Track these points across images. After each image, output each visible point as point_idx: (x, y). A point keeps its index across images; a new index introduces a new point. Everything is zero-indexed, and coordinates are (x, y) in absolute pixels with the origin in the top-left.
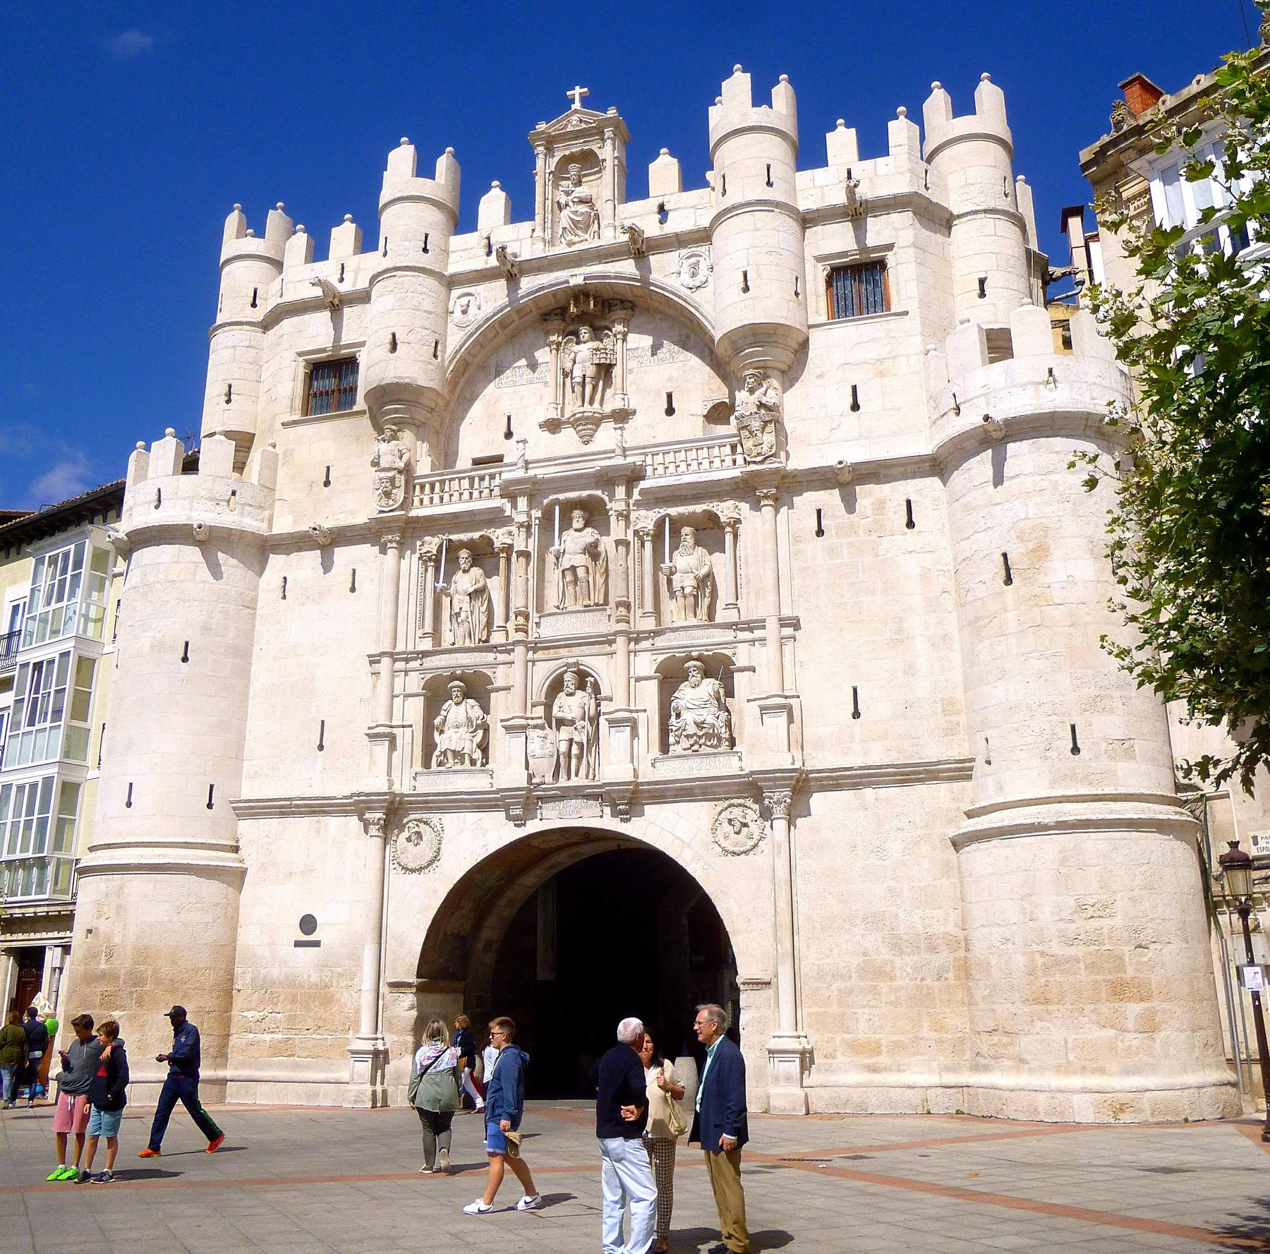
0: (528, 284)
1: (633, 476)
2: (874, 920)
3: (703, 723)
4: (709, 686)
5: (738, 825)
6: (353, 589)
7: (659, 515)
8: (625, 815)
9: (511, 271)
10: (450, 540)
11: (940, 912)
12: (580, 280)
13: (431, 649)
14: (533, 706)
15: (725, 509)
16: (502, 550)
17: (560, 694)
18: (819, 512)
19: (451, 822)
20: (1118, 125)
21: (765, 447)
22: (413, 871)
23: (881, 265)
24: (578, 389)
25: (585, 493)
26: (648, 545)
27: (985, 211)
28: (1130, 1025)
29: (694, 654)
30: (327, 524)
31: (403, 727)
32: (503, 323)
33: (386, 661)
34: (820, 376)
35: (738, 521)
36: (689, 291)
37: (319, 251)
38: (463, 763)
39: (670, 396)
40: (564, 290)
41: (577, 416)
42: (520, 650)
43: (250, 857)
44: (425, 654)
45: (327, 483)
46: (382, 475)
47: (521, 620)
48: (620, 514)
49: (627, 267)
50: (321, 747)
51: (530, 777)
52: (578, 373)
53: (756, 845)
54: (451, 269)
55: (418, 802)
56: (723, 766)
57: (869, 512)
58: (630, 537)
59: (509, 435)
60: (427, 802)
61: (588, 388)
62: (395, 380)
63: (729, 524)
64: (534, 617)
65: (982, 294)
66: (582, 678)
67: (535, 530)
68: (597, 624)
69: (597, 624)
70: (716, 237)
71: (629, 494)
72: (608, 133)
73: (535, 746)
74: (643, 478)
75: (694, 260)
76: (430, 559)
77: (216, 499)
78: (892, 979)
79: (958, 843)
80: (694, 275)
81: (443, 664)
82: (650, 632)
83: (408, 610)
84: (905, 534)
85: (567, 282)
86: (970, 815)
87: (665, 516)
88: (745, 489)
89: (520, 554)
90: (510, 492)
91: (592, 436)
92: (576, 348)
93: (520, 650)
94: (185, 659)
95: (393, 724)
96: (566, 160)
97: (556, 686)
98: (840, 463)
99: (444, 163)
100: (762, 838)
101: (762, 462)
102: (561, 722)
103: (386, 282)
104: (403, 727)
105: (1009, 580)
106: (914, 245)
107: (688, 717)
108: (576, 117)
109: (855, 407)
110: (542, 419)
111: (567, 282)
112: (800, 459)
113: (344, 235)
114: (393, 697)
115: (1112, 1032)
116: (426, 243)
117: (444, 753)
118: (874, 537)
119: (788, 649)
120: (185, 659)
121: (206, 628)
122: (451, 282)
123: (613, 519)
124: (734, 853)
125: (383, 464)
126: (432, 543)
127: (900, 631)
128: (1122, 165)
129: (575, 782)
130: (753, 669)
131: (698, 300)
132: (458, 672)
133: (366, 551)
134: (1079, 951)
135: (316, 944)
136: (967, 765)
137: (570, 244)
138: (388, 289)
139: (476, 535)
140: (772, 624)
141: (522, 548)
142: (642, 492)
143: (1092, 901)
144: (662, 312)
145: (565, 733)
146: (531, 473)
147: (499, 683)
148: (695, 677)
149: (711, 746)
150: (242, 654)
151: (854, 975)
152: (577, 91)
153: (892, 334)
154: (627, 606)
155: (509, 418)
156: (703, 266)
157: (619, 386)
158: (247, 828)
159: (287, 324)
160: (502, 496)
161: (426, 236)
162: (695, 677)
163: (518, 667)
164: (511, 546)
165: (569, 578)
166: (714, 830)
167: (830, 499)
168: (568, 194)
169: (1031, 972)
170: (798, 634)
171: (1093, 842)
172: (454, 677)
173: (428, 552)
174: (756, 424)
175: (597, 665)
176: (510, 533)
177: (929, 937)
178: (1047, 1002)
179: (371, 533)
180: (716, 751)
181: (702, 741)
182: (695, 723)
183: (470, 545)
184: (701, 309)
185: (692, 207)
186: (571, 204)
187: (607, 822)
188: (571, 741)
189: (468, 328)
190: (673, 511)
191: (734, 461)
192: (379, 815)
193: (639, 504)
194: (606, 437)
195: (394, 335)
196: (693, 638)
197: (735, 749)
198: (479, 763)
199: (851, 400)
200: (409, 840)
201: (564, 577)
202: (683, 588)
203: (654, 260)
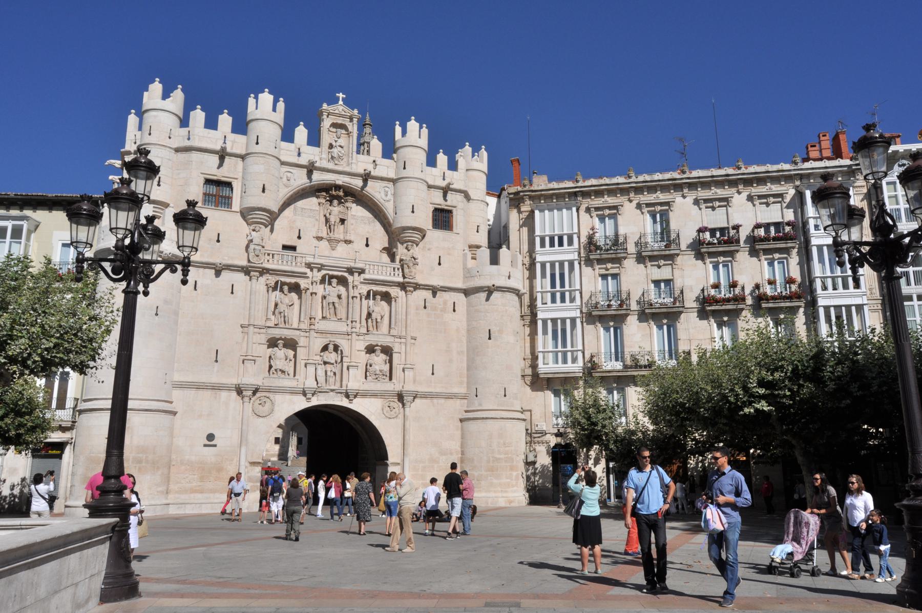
0: (317, 177)
1: (362, 271)
4: (383, 357)
6: (232, 293)
9: (311, 169)
12: (339, 182)
15: (394, 291)
19: (278, 398)
20: (525, 186)
23: (450, 212)
25: (340, 274)
27: (482, 201)
28: (514, 478)
30: (224, 262)
32: (303, 190)
33: (251, 328)
34: (429, 249)
37: (211, 123)
39: (367, 239)
42: (312, 332)
45: (218, 241)
46: (257, 247)
49: (358, 183)
51: (317, 384)
54: (283, 159)
55: (266, 389)
59: (299, 237)
61: (336, 227)
64: (317, 320)
65: (478, 232)
66: (336, 348)
67: (318, 283)
68: (343, 327)
69: (343, 327)
70: (399, 184)
72: (355, 120)
75: (387, 189)
77: (172, 240)
79: (461, 420)
80: (387, 195)
81: (276, 332)
86: (466, 411)
89: (312, 294)
90: (309, 266)
92: (330, 207)
93: (312, 332)
94: (157, 314)
96: (334, 125)
97: (325, 348)
99: (281, 105)
100: (399, 414)
102: (325, 363)
103: (260, 159)
105: (490, 338)
106: (463, 209)
108: (340, 107)
109: (440, 264)
110: (315, 235)
112: (420, 280)
113: (225, 120)
115: (509, 480)
117: (276, 370)
120: (157, 314)
121: (166, 302)
122: (283, 163)
125: (255, 241)
126: (272, 279)
128: (523, 199)
129: (333, 387)
130: (400, 353)
132: (283, 337)
133: (241, 276)
134: (502, 456)
135: (215, 446)
137: (336, 164)
140: (409, 338)
141: (314, 291)
142: (364, 280)
143: (507, 442)
144: (366, 203)
145: (329, 367)
147: (301, 344)
148: (378, 352)
150: (176, 314)
152: (341, 95)
155: (300, 230)
156: (389, 193)
158: (177, 394)
159: (195, 156)
162: (378, 352)
164: (308, 289)
165: (331, 306)
166: (383, 409)
167: (428, 294)
168: (336, 141)
169: (488, 461)
170: (416, 342)
171: (509, 424)
172: (280, 339)
175: (343, 343)
178: (493, 471)
179: (246, 271)
187: (344, 403)
189: (290, 188)
192: (250, 393)
193: (361, 283)
194: (341, 249)
195: (264, 185)
199: (438, 261)
200: (260, 404)
203: (370, 183)
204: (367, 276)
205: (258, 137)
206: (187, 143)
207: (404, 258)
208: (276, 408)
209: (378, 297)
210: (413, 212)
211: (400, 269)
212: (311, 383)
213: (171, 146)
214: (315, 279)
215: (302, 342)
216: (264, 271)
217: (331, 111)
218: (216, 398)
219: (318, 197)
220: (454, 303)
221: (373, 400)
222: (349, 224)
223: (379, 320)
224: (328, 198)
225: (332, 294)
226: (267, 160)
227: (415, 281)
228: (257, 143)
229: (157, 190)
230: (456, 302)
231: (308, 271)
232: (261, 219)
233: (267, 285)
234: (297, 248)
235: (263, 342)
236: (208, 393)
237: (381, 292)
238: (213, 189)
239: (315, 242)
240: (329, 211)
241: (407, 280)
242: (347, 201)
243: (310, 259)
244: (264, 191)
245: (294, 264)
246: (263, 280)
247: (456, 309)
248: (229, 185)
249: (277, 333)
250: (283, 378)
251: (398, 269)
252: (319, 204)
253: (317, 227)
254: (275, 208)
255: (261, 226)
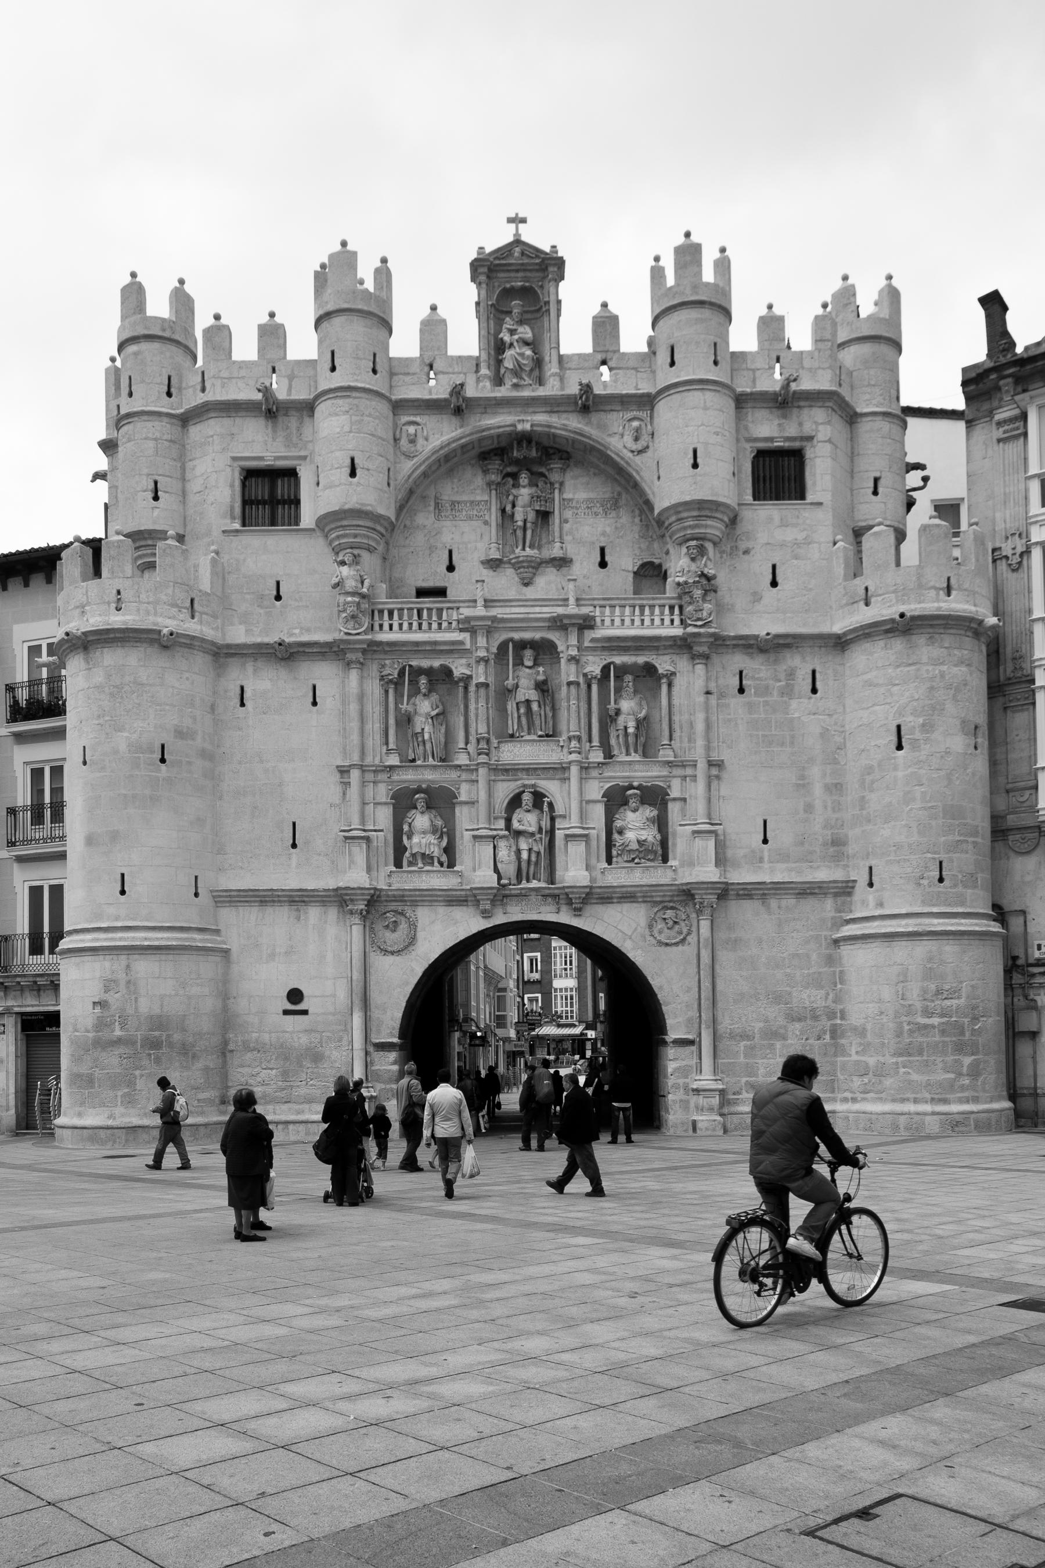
1: (586, 624)
2: (778, 998)
3: (644, 841)
5: (671, 923)
6: (315, 703)
7: (605, 662)
8: (578, 912)
10: (410, 666)
11: (823, 992)
12: (527, 427)
13: (398, 763)
14: (496, 818)
15: (663, 664)
16: (461, 680)
17: (518, 811)
18: (741, 673)
19: (423, 915)
21: (705, 614)
22: (392, 953)
24: (520, 533)
25: (537, 636)
26: (595, 688)
29: (635, 784)
31: (375, 831)
35: (673, 674)
36: (630, 455)
38: (432, 864)
40: (510, 434)
41: (521, 559)
42: (482, 771)
43: (233, 940)
44: (392, 768)
45: (278, 598)
47: (483, 745)
48: (572, 659)
50: (294, 846)
52: (519, 517)
53: (683, 940)
56: (657, 876)
57: (782, 676)
58: (581, 680)
60: (403, 896)
61: (529, 533)
62: (358, 506)
63: (666, 676)
64: (494, 742)
66: (538, 798)
71: (580, 639)
73: (503, 853)
74: (592, 627)
75: (635, 424)
76: (391, 681)
78: (785, 1038)
82: (599, 763)
83: (374, 726)
84: (810, 698)
85: (514, 425)
87: (610, 664)
88: (683, 645)
89: (478, 685)
90: (468, 626)
91: (532, 579)
92: (514, 491)
95: (367, 828)
97: (515, 802)
98: (768, 634)
100: (689, 934)
101: (701, 626)
102: (518, 833)
103: (340, 402)
104: (375, 831)
107: (631, 836)
111: (515, 426)
114: (364, 803)
116: (374, 362)
117: (414, 855)
118: (785, 699)
119: (715, 784)
122: (398, 406)
123: (563, 661)
124: (667, 945)
127: (802, 777)
129: (534, 884)
131: (639, 463)
132: (424, 786)
136: (850, 885)
138: (343, 409)
139: (436, 664)
140: (702, 765)
141: (482, 680)
142: (593, 640)
146: (493, 612)
147: (463, 797)
149: (649, 860)
151: (757, 1036)
153: (808, 522)
154: (579, 739)
157: (557, 534)
158: (228, 916)
160: (461, 630)
161: (375, 355)
163: (482, 784)
164: (470, 677)
165: (522, 710)
166: (650, 927)
168: (512, 332)
172: (419, 790)
173: (390, 674)
174: (698, 593)
175: (551, 787)
176: (469, 665)
177: (813, 1010)
180: (652, 864)
181: (642, 855)
182: (638, 841)
183: (429, 672)
184: (642, 474)
185: (633, 369)
186: (515, 344)
188: (530, 850)
189: (415, 460)
190: (618, 660)
191: (672, 621)
195: (353, 460)
196: (635, 771)
197: (671, 863)
198: (445, 864)
199: (769, 577)
200: (387, 927)
201: (518, 709)
202: (626, 728)
204: (599, 633)
205: (333, 353)
206: (201, 398)
207: (681, 580)
208: (421, 935)
209: (629, 678)
210: (695, 466)
211: (677, 611)
212: (485, 877)
213: (173, 412)
214: (482, 653)
215: (464, 793)
216: (373, 649)
217: (497, 262)
218: (298, 918)
219: (485, 472)
220: (814, 672)
221: (626, 907)
222: (557, 521)
223: (631, 730)
224: (509, 469)
225: (524, 682)
226: (356, 401)
227: (712, 630)
228: (333, 369)
229: (153, 508)
230: (818, 669)
231: (465, 637)
232: (355, 536)
233: (382, 678)
234: (448, 592)
235: (384, 800)
236: (280, 916)
237: (635, 664)
238: (260, 489)
239: (486, 573)
240: (511, 498)
241: (690, 630)
242: (552, 469)
243: (466, 612)
244: (353, 474)
245: (435, 626)
246: (373, 669)
247: (819, 685)
248: (291, 474)
249: (409, 777)
250: (428, 871)
251: (672, 608)
252: (489, 484)
253: (486, 538)
254: (387, 510)
255: (356, 552)
